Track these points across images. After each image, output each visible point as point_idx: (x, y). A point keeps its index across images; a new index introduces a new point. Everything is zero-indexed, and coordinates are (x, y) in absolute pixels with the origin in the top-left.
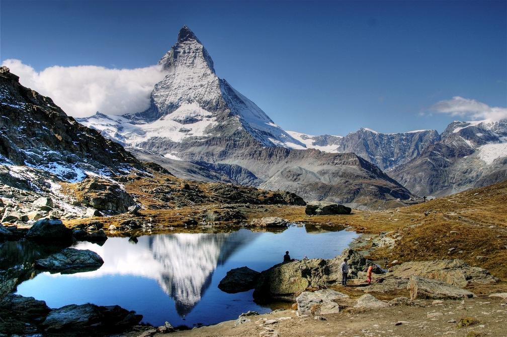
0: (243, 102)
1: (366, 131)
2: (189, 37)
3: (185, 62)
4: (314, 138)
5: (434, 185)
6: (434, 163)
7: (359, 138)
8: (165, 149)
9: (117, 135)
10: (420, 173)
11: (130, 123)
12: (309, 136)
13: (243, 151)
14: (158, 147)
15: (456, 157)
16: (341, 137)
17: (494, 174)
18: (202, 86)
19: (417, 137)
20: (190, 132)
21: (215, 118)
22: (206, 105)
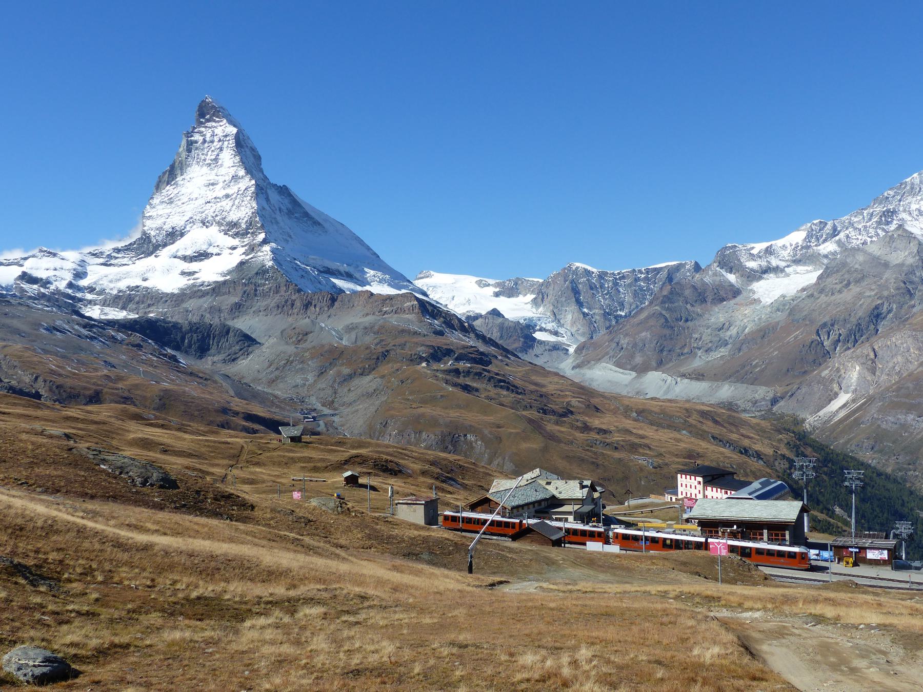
0: (319, 224)
1: (577, 268)
2: (214, 115)
3: (203, 157)
4: (497, 285)
5: (665, 353)
6: (667, 316)
7: (566, 281)
8: (149, 306)
9: (70, 285)
10: (644, 334)
11: (102, 264)
12: (491, 281)
13: (269, 300)
14: (138, 303)
15: (709, 304)
16: (541, 281)
17: (760, 330)
18: (227, 196)
19: (664, 274)
20: (196, 276)
21: (243, 250)
22: (232, 228)
